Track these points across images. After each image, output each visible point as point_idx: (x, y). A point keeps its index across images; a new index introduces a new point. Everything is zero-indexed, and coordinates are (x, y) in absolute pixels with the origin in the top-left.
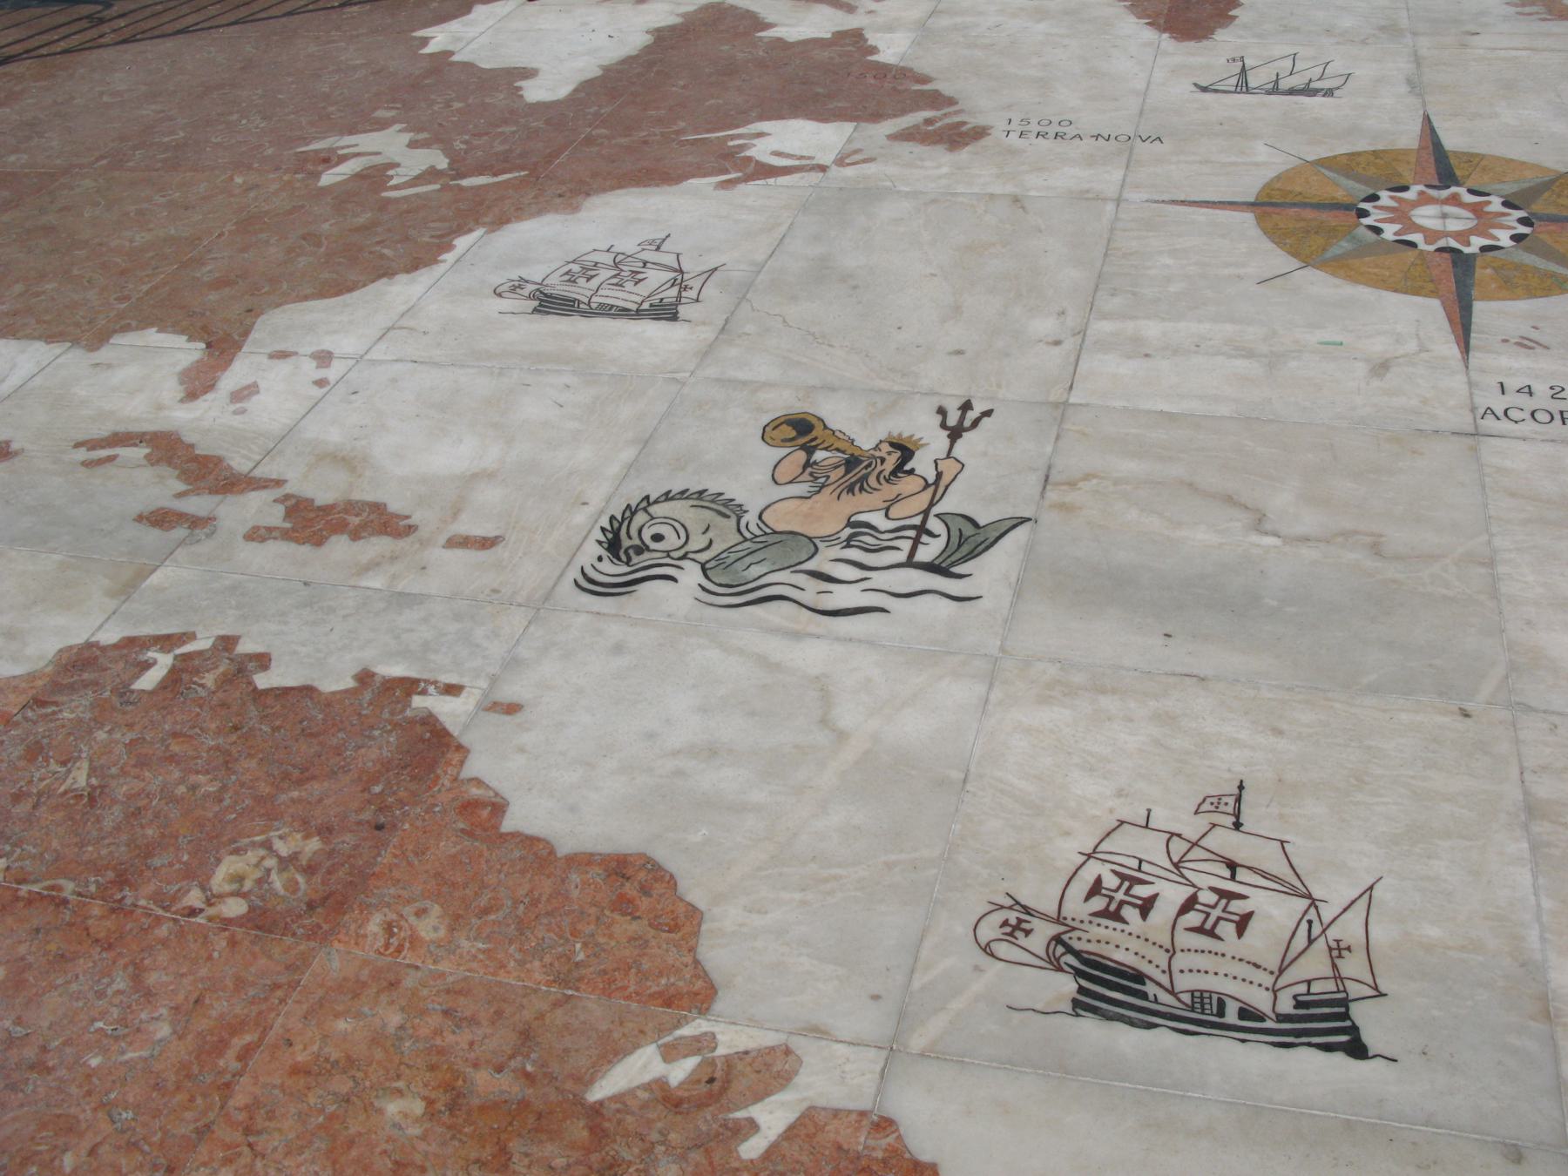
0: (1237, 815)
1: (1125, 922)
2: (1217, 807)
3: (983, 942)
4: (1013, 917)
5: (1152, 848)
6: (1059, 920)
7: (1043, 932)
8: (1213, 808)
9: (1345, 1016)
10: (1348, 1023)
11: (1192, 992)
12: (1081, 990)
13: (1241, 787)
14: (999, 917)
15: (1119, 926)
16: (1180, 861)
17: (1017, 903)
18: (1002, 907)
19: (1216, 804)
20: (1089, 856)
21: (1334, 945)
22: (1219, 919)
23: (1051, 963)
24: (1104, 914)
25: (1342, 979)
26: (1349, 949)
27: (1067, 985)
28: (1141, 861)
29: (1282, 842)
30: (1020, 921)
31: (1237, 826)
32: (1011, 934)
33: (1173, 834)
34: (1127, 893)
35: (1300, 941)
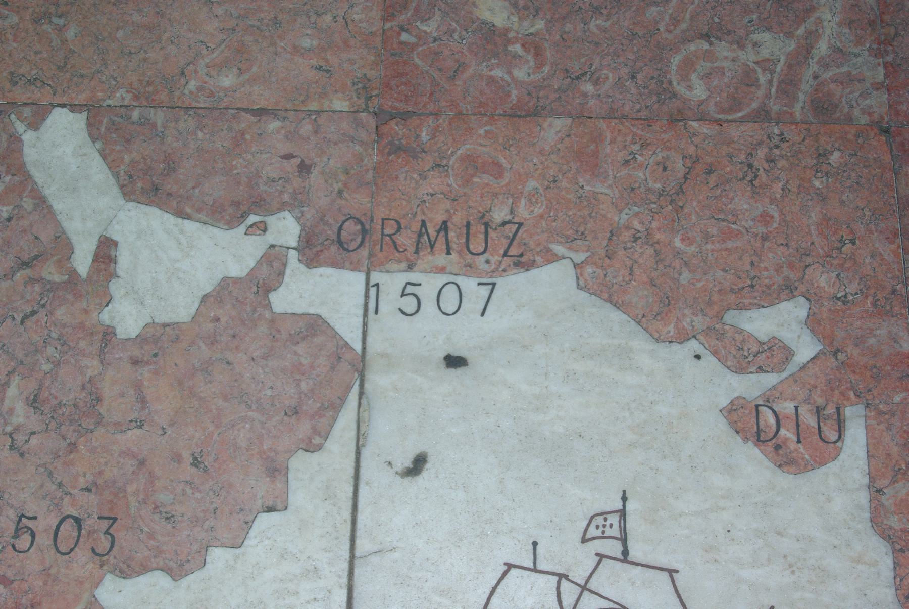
2: (603, 532)
8: (598, 533)
13: (624, 499)
19: (601, 529)
29: (672, 572)
31: (625, 552)
33: (562, 576)
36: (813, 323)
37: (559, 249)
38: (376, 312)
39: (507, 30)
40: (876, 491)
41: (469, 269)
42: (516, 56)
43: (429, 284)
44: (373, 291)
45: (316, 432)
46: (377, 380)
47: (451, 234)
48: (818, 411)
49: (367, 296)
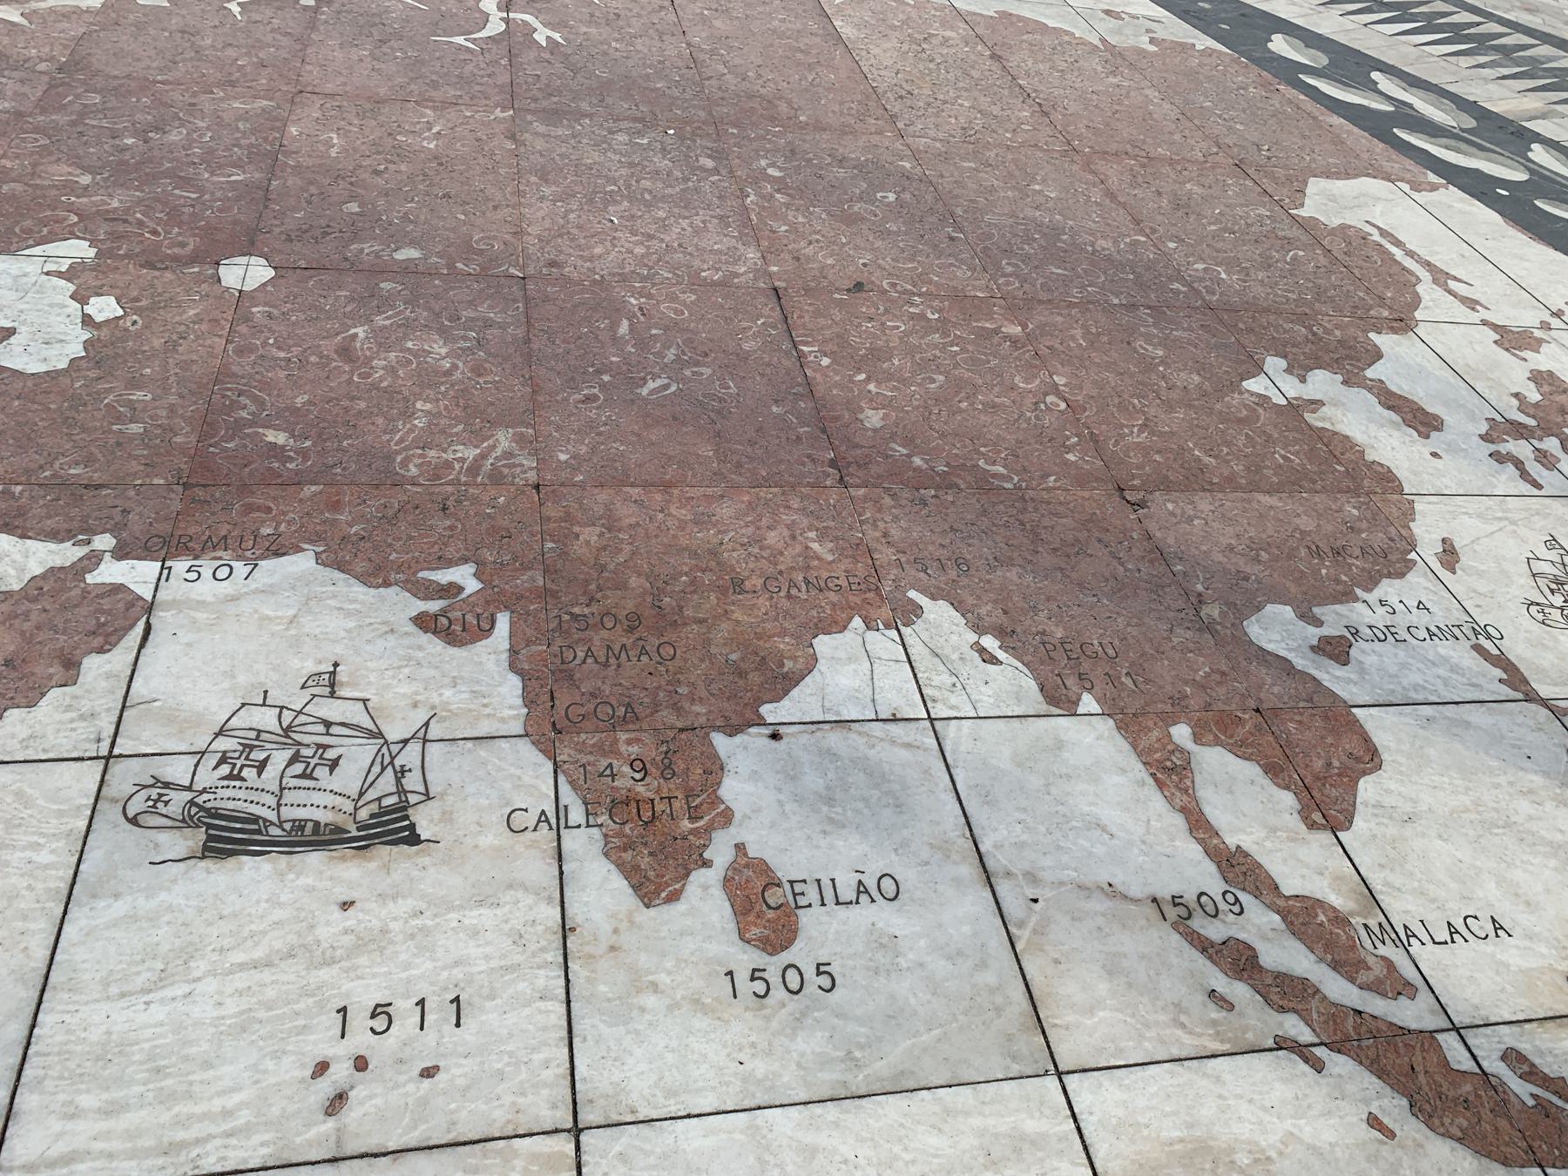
0: (332, 685)
1: (243, 780)
3: (131, 814)
4: (154, 793)
5: (266, 719)
6: (189, 788)
7: (179, 799)
9: (406, 817)
10: (407, 823)
11: (294, 821)
12: (210, 838)
14: (144, 794)
15: (238, 784)
16: (290, 726)
17: (158, 781)
18: (145, 787)
20: (217, 735)
21: (398, 769)
22: (316, 765)
23: (183, 821)
24: (230, 777)
25: (406, 792)
26: (410, 770)
27: (196, 838)
28: (259, 731)
29: (365, 701)
30: (161, 795)
32: (154, 806)
33: (282, 708)
34: (247, 758)
35: (377, 769)
36: (476, 575)
37: (306, 546)
38: (167, 580)
39: (283, 447)
40: (513, 652)
41: (239, 558)
42: (289, 457)
43: (207, 568)
44: (165, 572)
45: (107, 642)
46: (161, 619)
47: (229, 541)
48: (478, 616)
49: (161, 574)
